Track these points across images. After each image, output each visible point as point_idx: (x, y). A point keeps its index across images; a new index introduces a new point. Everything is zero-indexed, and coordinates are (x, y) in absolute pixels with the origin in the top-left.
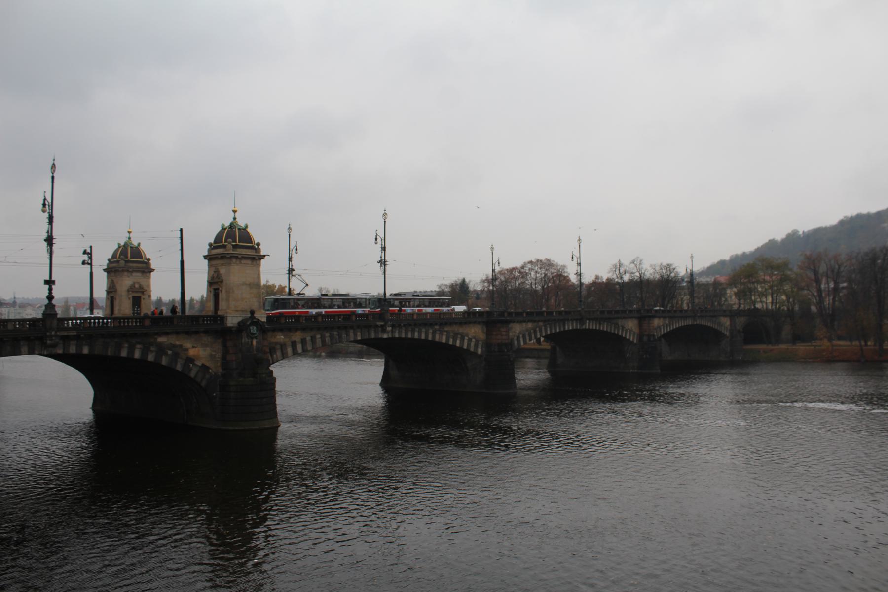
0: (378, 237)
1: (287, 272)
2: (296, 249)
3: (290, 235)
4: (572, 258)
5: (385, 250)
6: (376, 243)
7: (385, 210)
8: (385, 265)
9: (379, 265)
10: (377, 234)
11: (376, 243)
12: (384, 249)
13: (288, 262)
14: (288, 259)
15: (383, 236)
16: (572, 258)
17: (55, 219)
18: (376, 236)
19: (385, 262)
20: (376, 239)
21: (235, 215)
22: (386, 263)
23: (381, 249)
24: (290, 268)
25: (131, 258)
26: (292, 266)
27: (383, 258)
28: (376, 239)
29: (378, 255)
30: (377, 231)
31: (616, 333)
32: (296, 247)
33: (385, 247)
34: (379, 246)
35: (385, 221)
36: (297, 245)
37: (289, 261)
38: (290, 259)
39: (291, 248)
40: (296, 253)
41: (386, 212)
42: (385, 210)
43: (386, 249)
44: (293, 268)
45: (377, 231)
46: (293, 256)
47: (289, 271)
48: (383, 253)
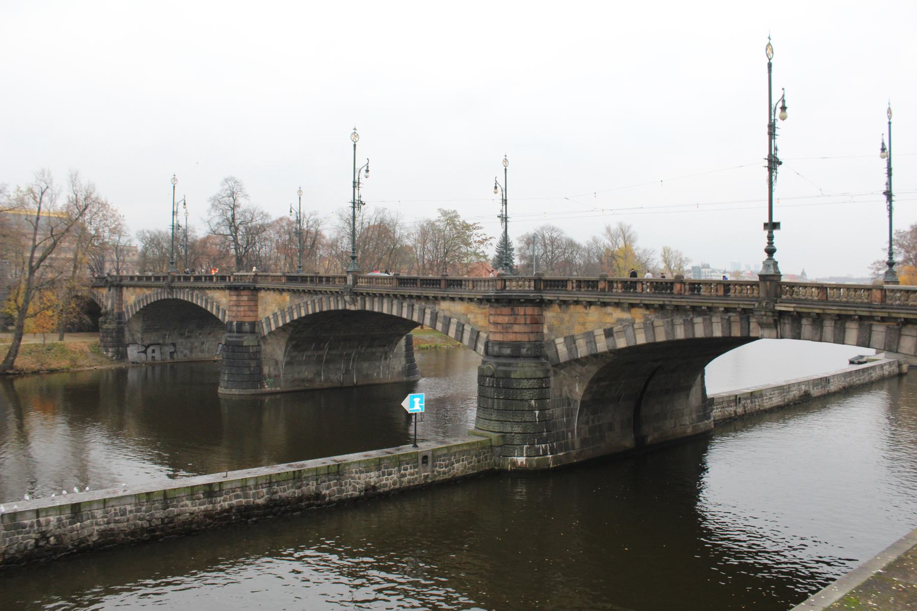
0: (497, 185)
1: (352, 205)
2: (367, 171)
3: (355, 146)
5: (506, 204)
6: (496, 193)
8: (506, 221)
9: (499, 220)
11: (496, 193)
12: (505, 202)
13: (353, 189)
14: (352, 184)
15: (504, 187)
17: (893, 172)
19: (506, 218)
20: (496, 188)
22: (508, 219)
23: (501, 201)
24: (357, 198)
27: (504, 213)
28: (496, 188)
29: (498, 208)
33: (506, 200)
34: (499, 196)
37: (354, 187)
38: (356, 184)
43: (508, 202)
47: (354, 203)
48: (504, 207)
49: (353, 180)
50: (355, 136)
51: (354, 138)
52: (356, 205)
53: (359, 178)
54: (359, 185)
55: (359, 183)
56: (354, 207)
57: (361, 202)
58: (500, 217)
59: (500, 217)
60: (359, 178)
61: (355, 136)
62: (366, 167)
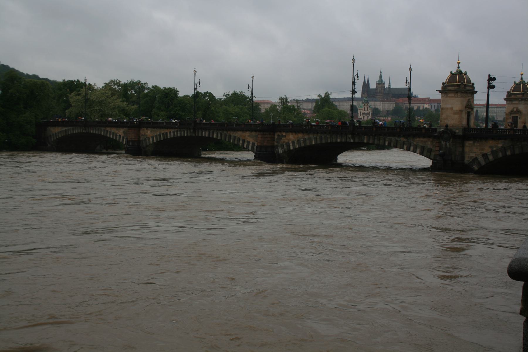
1: (351, 93)
2: (358, 77)
3: (353, 65)
4: (248, 88)
7: (410, 66)
10: (407, 79)
14: (352, 83)
15: (409, 82)
16: (248, 88)
20: (406, 83)
21: (522, 76)
24: (354, 89)
25: (458, 83)
26: (355, 88)
31: (114, 138)
32: (358, 75)
38: (354, 83)
39: (354, 74)
40: (358, 80)
42: (410, 66)
46: (355, 81)
53: (355, 80)
54: (354, 83)
56: (353, 94)
57: (355, 91)
60: (355, 80)
62: (357, 75)
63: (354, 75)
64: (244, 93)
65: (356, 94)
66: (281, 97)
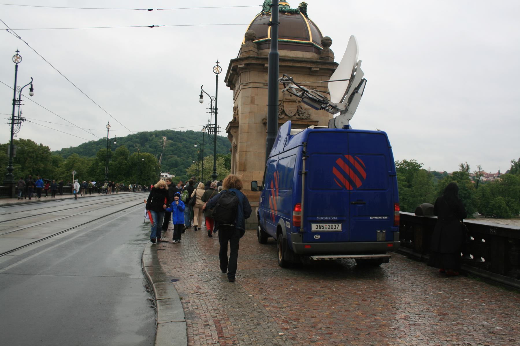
0: (204, 94)
2: (32, 89)
3: (17, 66)
7: (218, 62)
10: (202, 90)
13: (12, 106)
14: (12, 102)
18: (202, 92)
19: (216, 128)
20: (201, 96)
23: (209, 111)
24: (16, 114)
27: (213, 122)
28: (201, 96)
30: (203, 86)
32: (32, 85)
33: (216, 109)
35: (217, 77)
36: (33, 83)
37: (14, 104)
40: (31, 96)
41: (219, 64)
42: (218, 62)
44: (22, 116)
45: (203, 86)
47: (13, 120)
49: (13, 98)
50: (18, 58)
51: (16, 60)
52: (15, 122)
53: (20, 96)
54: (19, 102)
55: (20, 100)
56: (13, 124)
58: (207, 127)
59: (207, 127)
60: (20, 96)
61: (18, 58)
63: (17, 85)
64: (416, 162)
65: (23, 123)
66: (462, 164)
